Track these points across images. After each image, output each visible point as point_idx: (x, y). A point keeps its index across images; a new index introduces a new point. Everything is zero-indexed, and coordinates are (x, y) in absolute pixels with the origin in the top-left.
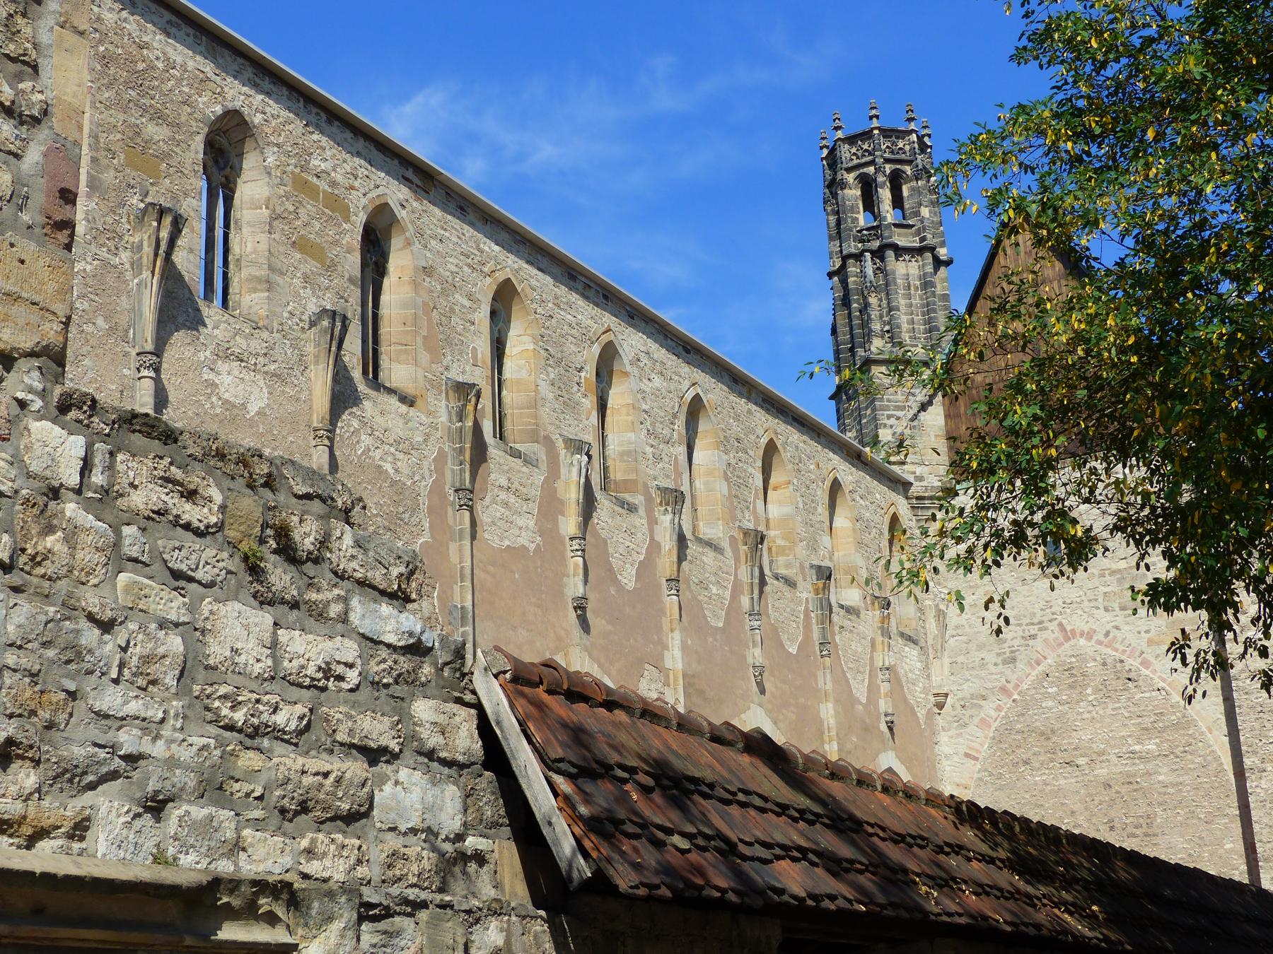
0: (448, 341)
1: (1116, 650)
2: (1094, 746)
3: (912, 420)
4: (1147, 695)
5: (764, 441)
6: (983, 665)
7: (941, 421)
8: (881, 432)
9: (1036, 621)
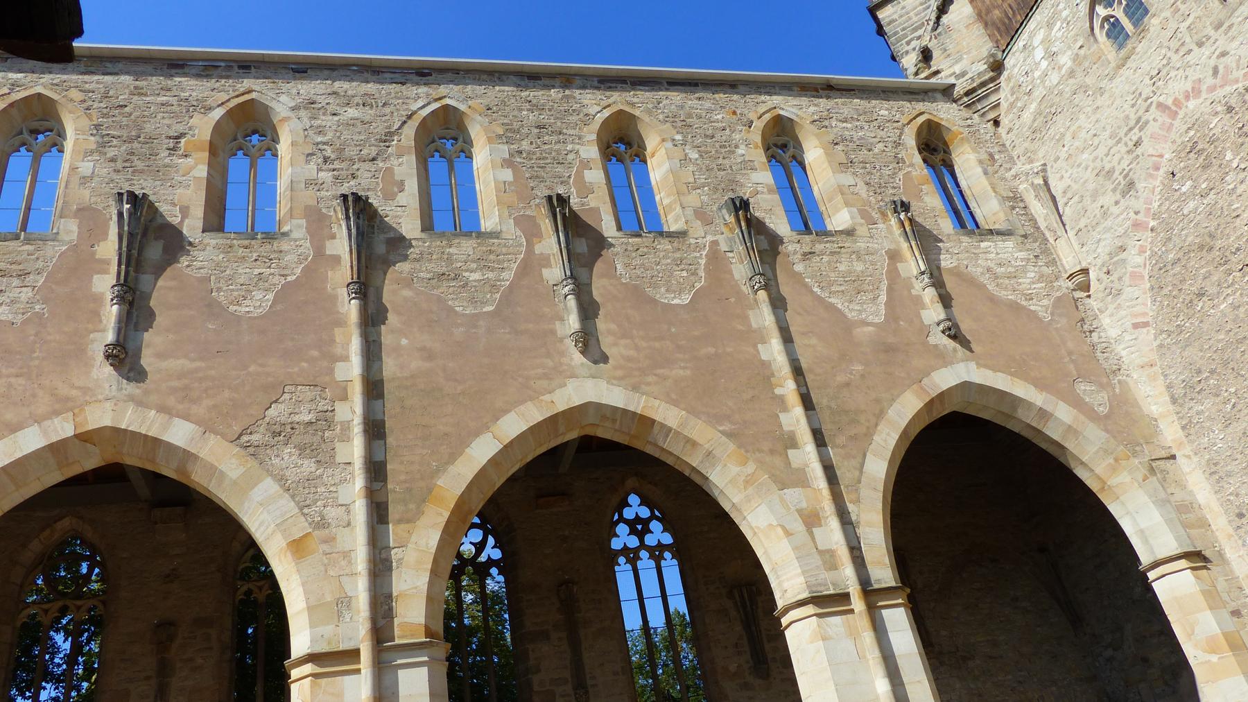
1: (1237, 81)
3: (935, 29)
6: (1105, 214)
9: (1132, 123)
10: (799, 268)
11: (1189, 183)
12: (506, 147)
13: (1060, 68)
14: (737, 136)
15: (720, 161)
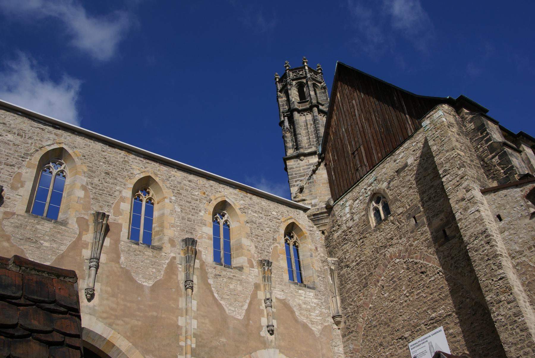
2: (411, 322)
3: (308, 180)
4: (433, 279)
10: (211, 281)
12: (85, 179)
13: (354, 221)
14: (201, 206)
15: (190, 216)
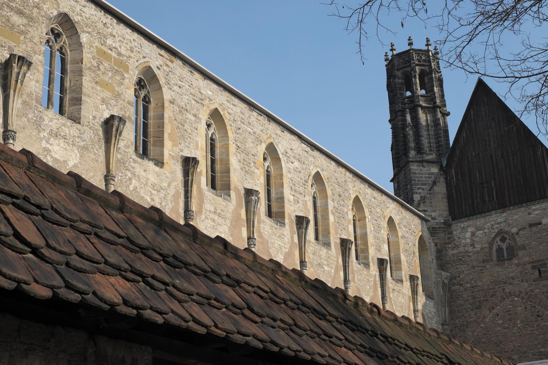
0: (183, 137)
2: (521, 349)
3: (430, 190)
5: (353, 197)
7: (444, 190)
8: (415, 196)
11: (501, 321)
